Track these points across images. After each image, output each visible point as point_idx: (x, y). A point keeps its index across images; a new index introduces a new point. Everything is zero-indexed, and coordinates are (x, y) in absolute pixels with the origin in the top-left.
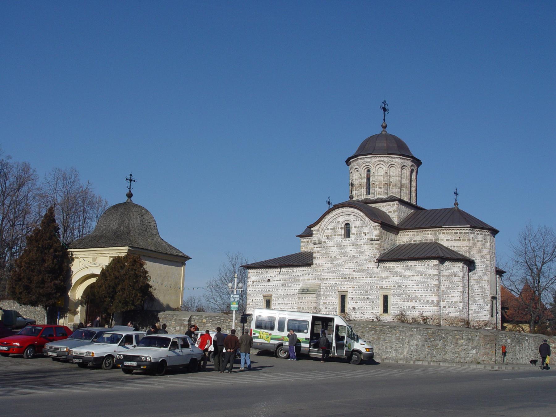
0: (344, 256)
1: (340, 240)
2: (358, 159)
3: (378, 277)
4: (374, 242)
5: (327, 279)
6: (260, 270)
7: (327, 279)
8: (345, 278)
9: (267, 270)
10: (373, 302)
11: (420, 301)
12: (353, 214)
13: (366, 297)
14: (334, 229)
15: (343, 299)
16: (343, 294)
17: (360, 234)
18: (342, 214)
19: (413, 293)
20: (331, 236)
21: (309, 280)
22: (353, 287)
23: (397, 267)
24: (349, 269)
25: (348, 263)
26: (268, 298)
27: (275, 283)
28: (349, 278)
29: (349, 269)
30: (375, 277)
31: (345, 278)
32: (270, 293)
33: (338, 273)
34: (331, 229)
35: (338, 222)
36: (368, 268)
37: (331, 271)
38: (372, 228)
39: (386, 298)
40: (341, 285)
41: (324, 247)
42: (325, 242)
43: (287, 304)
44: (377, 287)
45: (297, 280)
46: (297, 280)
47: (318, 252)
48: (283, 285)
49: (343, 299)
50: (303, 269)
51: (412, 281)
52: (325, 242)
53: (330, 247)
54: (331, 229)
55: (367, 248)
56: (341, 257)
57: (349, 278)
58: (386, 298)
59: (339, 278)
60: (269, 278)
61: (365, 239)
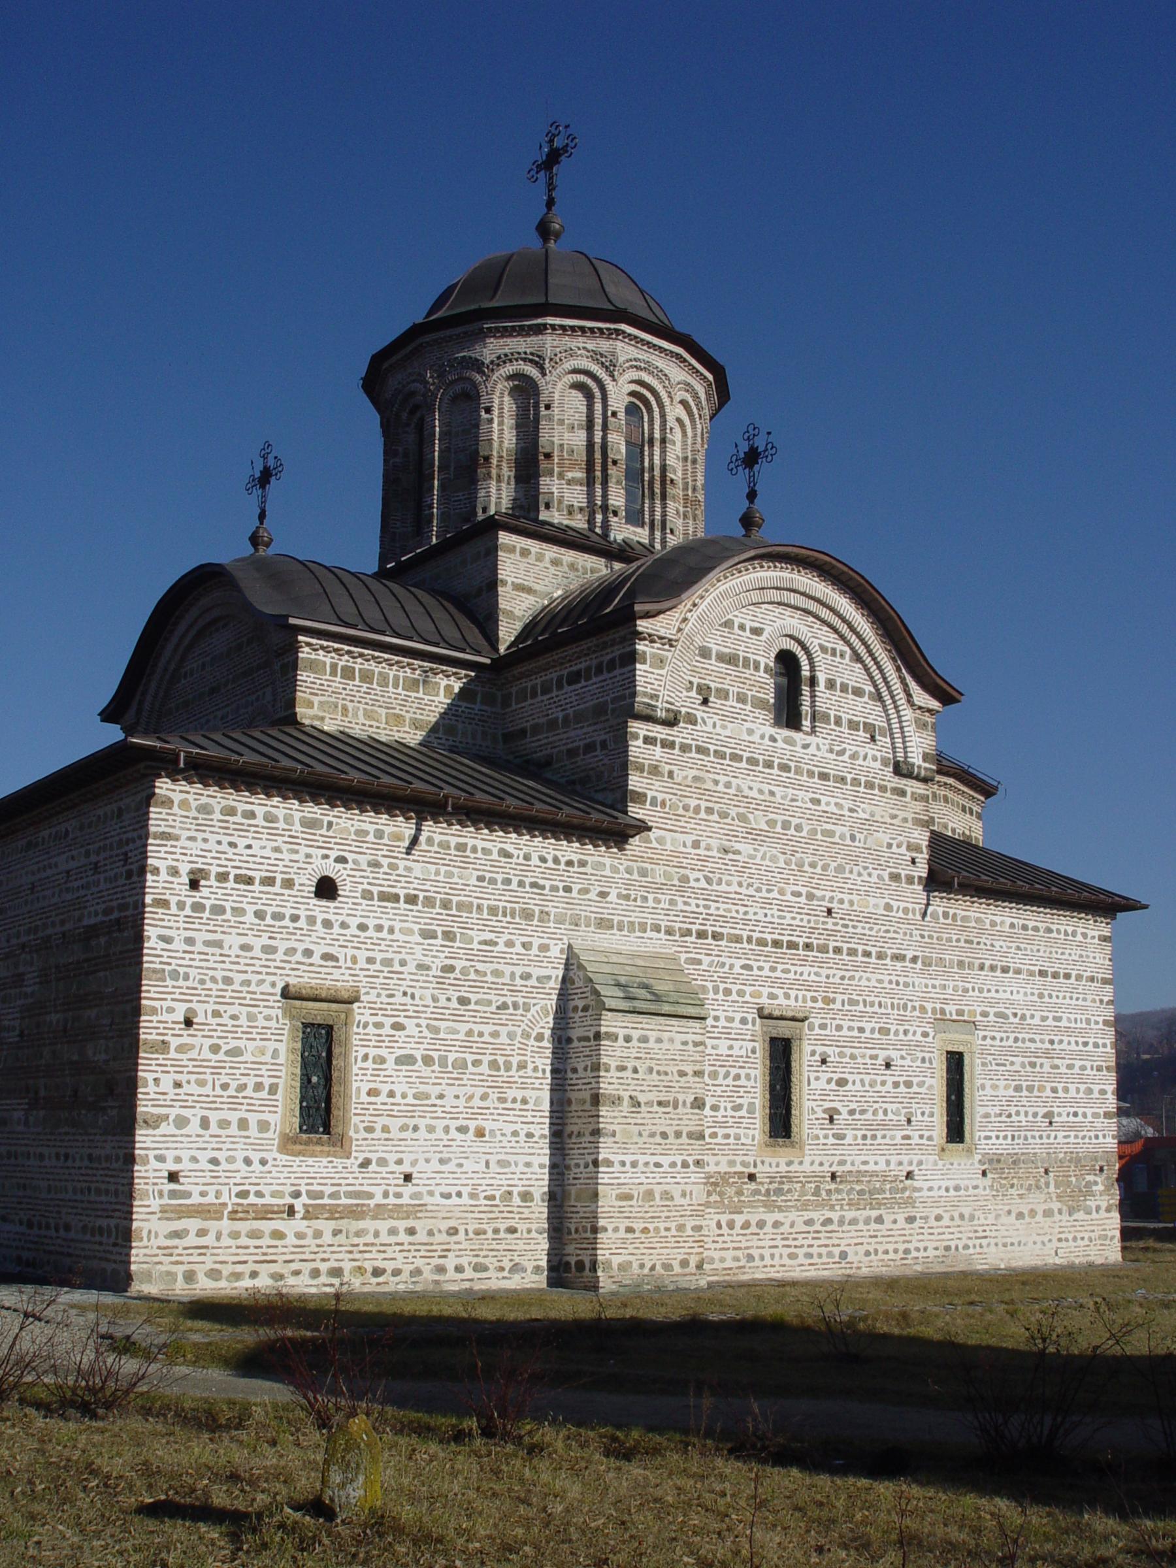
0: (786, 825)
1: (759, 730)
2: (540, 330)
3: (927, 963)
4: (912, 787)
5: (701, 935)
6: (261, 805)
7: (701, 935)
8: (792, 945)
9: (313, 810)
10: (908, 1084)
11: (1066, 1090)
12: (825, 613)
13: (882, 1055)
14: (730, 659)
15: (781, 1054)
16: (783, 1029)
17: (853, 725)
18: (775, 595)
19: (1047, 1054)
20: (723, 694)
21: (604, 924)
22: (828, 1001)
23: (993, 924)
24: (810, 897)
25: (800, 865)
26: (318, 1012)
27: (375, 914)
28: (808, 946)
29: (810, 897)
30: (914, 959)
31: (792, 945)
32: (337, 979)
33: (755, 912)
34: (721, 658)
35: (757, 631)
36: (888, 907)
37: (725, 896)
38: (908, 714)
39: (956, 1063)
40: (774, 982)
41: (685, 748)
42: (692, 720)
43: (461, 1065)
44: (923, 1009)
45: (527, 915)
46: (527, 915)
47: (655, 770)
48: (429, 935)
49: (781, 1054)
50: (569, 850)
51: (1041, 996)
52: (692, 720)
53: (720, 755)
54: (721, 658)
55: (881, 806)
56: (771, 823)
57: (808, 946)
58: (956, 1063)
59: (762, 942)
60: (331, 869)
61: (872, 760)
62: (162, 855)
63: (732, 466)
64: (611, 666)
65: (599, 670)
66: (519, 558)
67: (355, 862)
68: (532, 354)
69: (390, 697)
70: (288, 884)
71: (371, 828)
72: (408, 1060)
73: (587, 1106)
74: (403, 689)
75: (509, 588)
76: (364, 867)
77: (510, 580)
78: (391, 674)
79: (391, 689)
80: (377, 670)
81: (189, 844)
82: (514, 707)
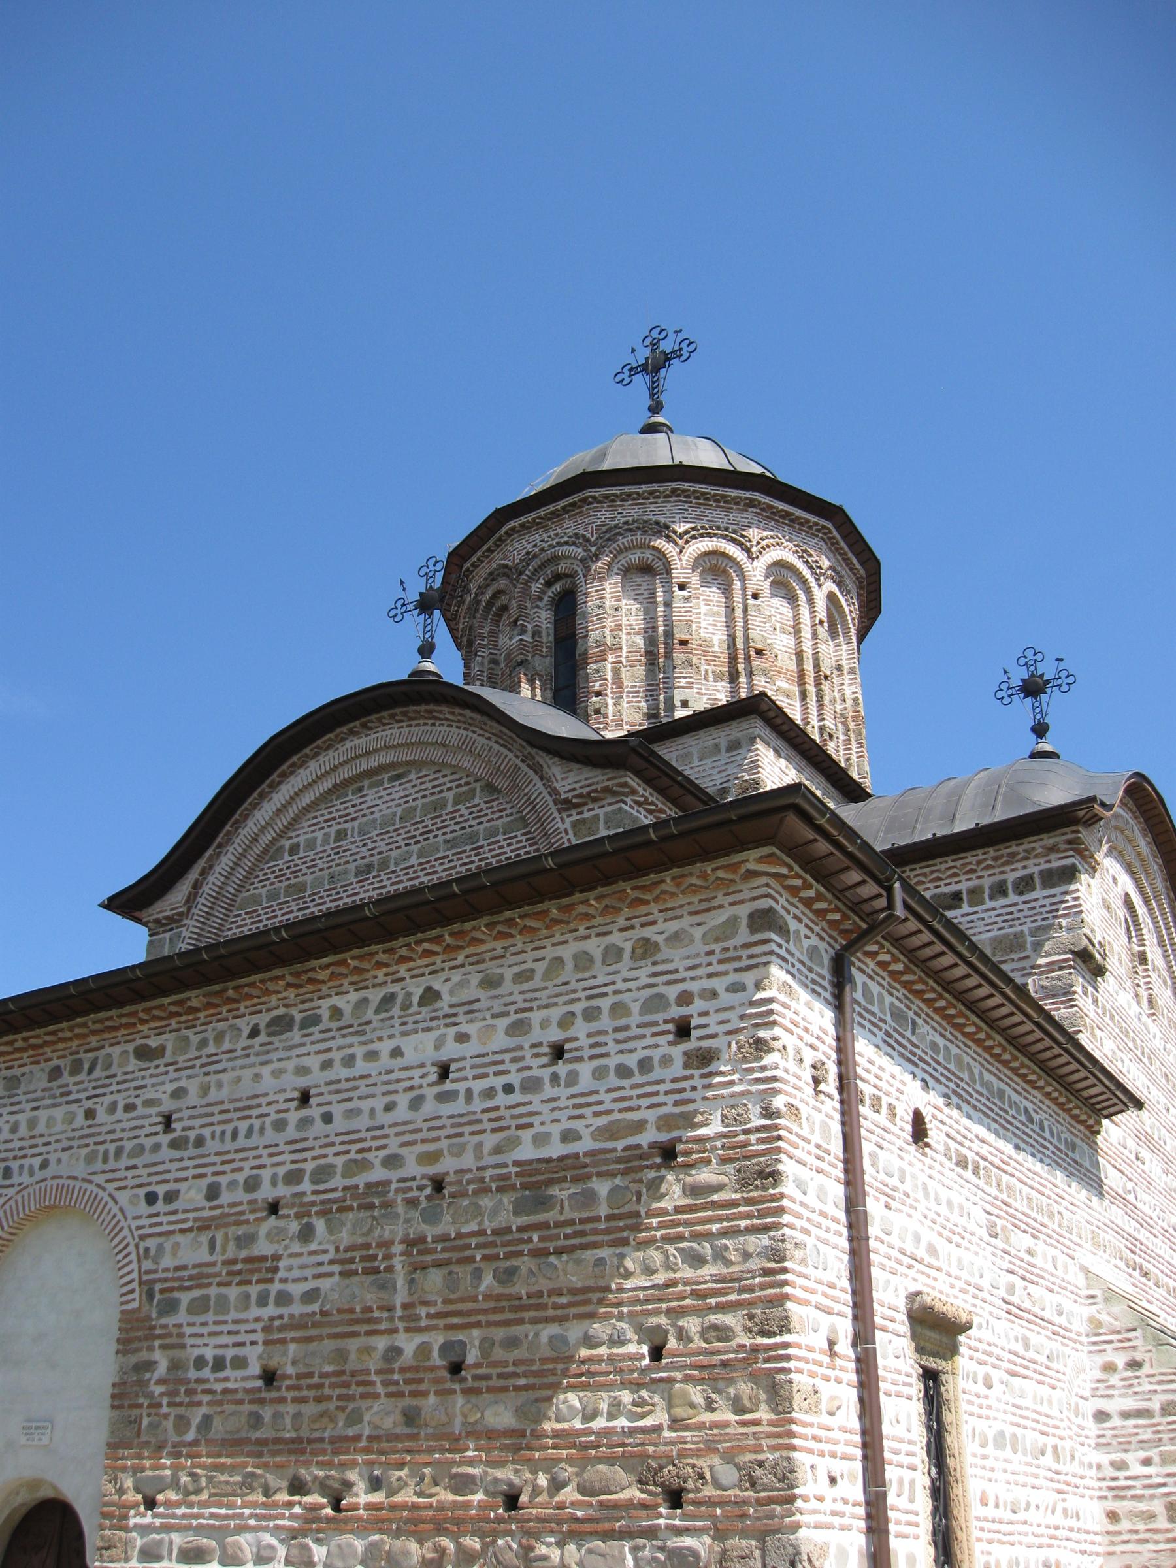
63: (1000, 694)
64: (1025, 885)
65: (1000, 890)
72: (1000, 1440)
73: (1162, 1523)
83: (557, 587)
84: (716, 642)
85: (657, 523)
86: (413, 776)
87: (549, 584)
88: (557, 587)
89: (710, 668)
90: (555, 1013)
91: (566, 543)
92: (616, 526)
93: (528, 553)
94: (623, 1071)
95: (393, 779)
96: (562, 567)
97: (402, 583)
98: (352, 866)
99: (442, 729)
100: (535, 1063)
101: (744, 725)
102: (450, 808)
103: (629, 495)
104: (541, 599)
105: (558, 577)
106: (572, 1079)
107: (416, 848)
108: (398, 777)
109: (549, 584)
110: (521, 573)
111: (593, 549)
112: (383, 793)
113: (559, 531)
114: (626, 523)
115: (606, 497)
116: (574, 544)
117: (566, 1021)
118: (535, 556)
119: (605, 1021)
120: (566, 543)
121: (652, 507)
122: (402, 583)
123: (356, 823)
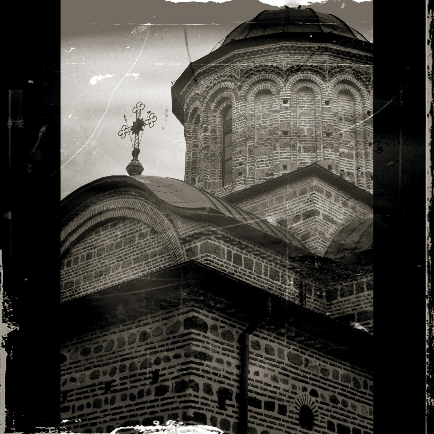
62: (200, 373)
66: (325, 197)
67: (323, 397)
68: (316, 67)
69: (263, 282)
70: (283, 410)
71: (331, 368)
74: (271, 277)
75: (321, 217)
76: (328, 401)
77: (321, 212)
78: (263, 264)
79: (263, 276)
80: (255, 260)
81: (217, 365)
82: (339, 299)
83: (224, 104)
84: (306, 130)
85: (272, 66)
86: (121, 225)
87: (219, 103)
88: (224, 104)
89: (302, 146)
90: (108, 368)
91: (226, 80)
92: (251, 70)
93: (208, 87)
94: (132, 397)
95: (112, 226)
96: (225, 94)
97: (125, 117)
98: (93, 273)
99: (131, 200)
100: (99, 392)
101: (308, 181)
102: (137, 242)
103: (257, 51)
104: (215, 111)
105: (224, 99)
106: (113, 400)
107: (121, 263)
108: (115, 225)
109: (219, 103)
110: (205, 98)
111: (239, 84)
112: (108, 234)
113: (222, 74)
114: (256, 67)
115: (245, 54)
116: (230, 80)
117: (113, 373)
118: (211, 88)
119: (127, 373)
120: (226, 80)
121: (270, 57)
122: (125, 117)
123: (96, 250)
